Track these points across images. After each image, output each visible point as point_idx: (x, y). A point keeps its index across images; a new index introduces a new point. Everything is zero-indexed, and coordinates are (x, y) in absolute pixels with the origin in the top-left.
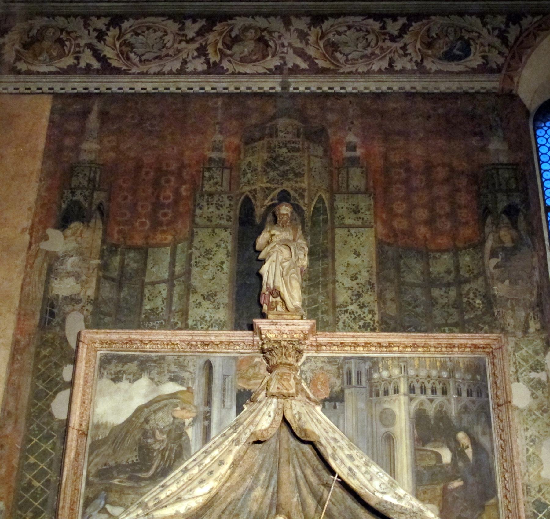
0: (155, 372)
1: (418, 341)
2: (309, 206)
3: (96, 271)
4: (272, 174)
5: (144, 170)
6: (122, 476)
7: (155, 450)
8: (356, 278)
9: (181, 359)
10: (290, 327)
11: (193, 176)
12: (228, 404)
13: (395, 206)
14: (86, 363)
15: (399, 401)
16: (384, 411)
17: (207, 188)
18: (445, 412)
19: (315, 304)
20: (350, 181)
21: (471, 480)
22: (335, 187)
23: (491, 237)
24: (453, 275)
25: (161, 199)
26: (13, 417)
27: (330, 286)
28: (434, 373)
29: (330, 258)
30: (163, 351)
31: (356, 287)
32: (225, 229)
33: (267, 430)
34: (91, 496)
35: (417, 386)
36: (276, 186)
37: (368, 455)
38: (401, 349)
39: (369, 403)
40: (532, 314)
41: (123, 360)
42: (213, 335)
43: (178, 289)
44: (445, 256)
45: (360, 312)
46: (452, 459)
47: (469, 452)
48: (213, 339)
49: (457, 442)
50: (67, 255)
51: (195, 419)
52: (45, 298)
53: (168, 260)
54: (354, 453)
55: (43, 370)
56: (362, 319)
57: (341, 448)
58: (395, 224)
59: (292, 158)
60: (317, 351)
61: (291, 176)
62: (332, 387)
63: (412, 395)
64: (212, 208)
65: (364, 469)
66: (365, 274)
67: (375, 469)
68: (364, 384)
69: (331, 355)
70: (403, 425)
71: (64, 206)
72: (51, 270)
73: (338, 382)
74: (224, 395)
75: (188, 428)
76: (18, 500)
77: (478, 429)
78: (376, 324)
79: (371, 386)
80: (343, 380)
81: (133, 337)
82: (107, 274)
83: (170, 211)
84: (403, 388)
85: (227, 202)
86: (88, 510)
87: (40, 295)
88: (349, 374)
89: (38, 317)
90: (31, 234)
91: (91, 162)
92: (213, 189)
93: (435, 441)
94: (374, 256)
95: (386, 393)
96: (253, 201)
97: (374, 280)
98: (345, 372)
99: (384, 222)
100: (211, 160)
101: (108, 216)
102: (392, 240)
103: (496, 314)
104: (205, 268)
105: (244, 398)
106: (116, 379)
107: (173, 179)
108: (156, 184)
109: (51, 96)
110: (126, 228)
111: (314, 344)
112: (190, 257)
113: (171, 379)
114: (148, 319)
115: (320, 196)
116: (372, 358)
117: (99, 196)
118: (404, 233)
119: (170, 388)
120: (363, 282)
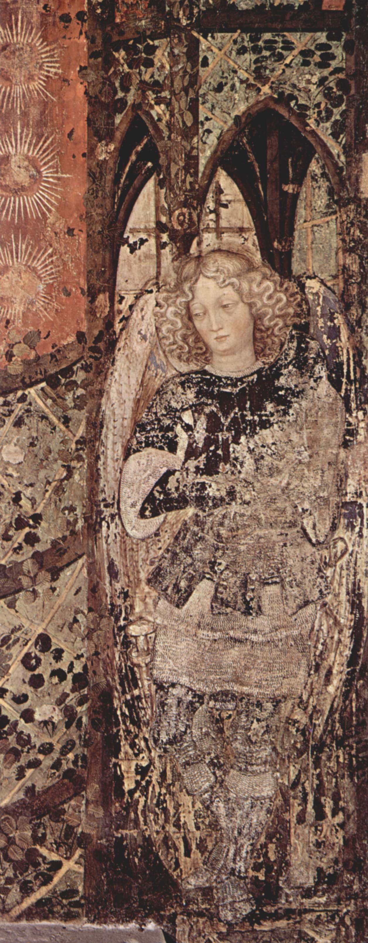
103: (128, 785)
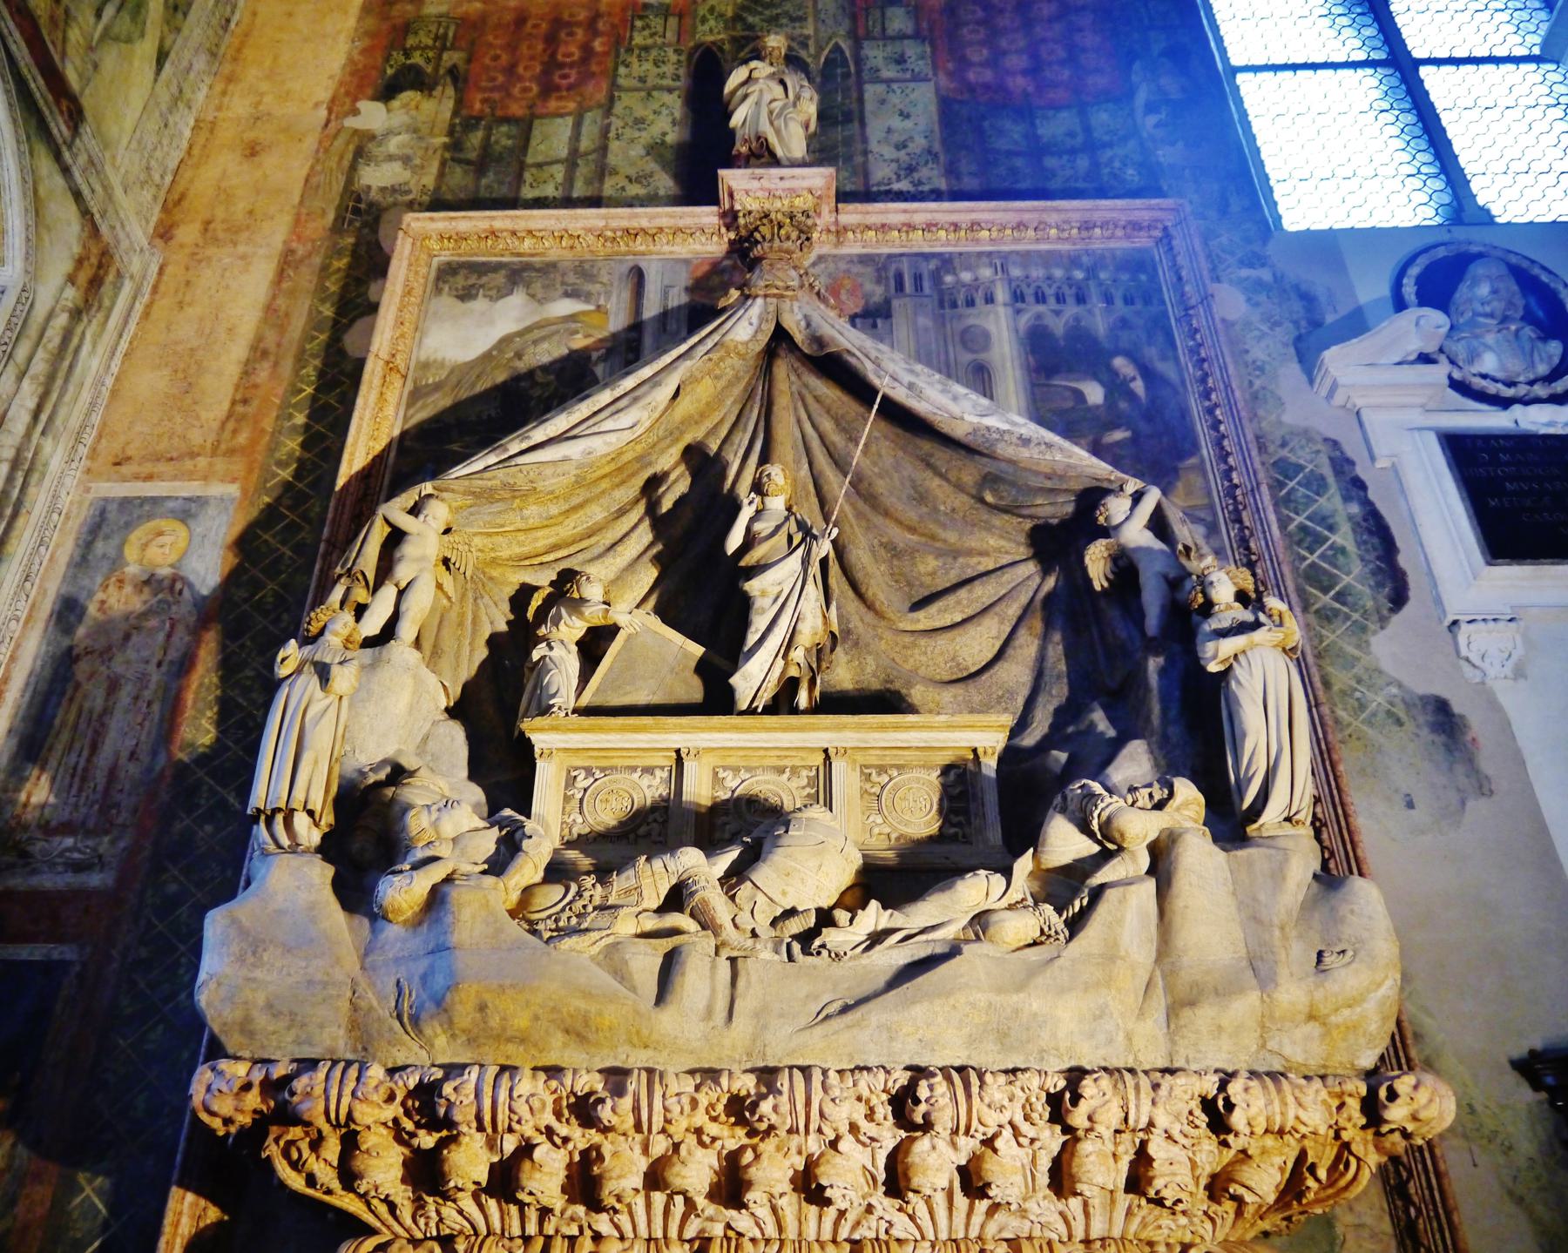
0: (537, 287)
1: (1026, 217)
2: (817, 57)
3: (439, 152)
5: (530, 24)
8: (905, 147)
9: (587, 266)
10: (787, 184)
11: (613, 26)
13: (968, 51)
14: (410, 265)
15: (996, 313)
16: (965, 331)
17: (638, 39)
20: (887, 23)
21: (1144, 427)
22: (861, 32)
24: (1080, 139)
26: (272, 358)
27: (859, 159)
29: (856, 124)
30: (554, 251)
31: (907, 158)
32: (670, 90)
33: (746, 343)
35: (1029, 293)
37: (940, 371)
38: (995, 234)
39: (941, 321)
42: (643, 217)
46: (1106, 397)
47: (1138, 386)
48: (644, 223)
53: (568, 133)
54: (919, 367)
57: (893, 360)
58: (971, 76)
63: (1019, 305)
64: (648, 66)
65: (939, 387)
67: (960, 389)
69: (865, 251)
70: (1007, 349)
71: (390, 72)
72: (359, 153)
75: (596, 364)
76: (266, 481)
77: (1151, 353)
79: (941, 293)
80: (887, 286)
81: (498, 224)
82: (461, 156)
84: (1001, 294)
85: (674, 58)
88: (899, 278)
89: (331, 216)
90: (330, 110)
91: (441, 16)
92: (650, 41)
93: (1070, 370)
94: (936, 118)
95: (971, 303)
97: (937, 147)
99: (950, 74)
101: (466, 80)
102: (966, 96)
106: (466, 295)
108: (551, 40)
110: (496, 96)
111: (833, 228)
113: (567, 295)
117: (451, 58)
118: (987, 87)
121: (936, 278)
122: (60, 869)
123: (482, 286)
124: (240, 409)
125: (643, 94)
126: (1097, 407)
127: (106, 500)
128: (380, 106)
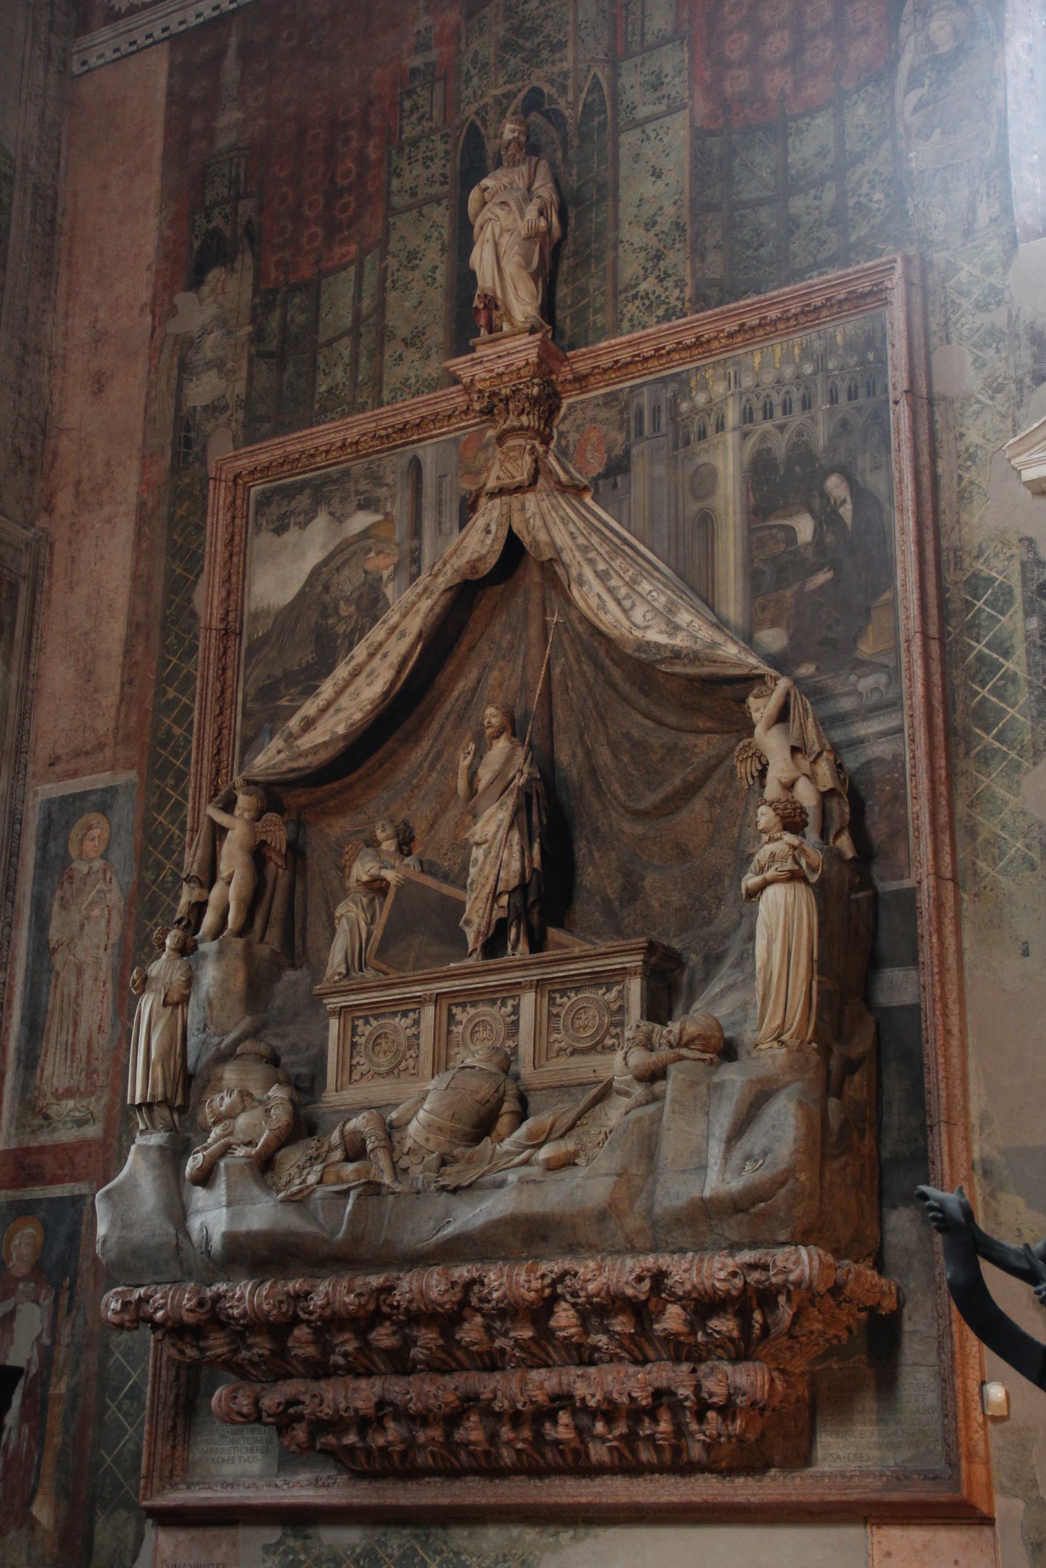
4: (514, 62)
6: (292, 691)
7: (338, 636)
8: (654, 223)
9: (374, 467)
12: (446, 525)
15: (725, 442)
17: (409, 132)
18: (806, 443)
19: (584, 297)
20: (647, 23)
23: (911, 45)
25: (339, 180)
28: (788, 372)
31: (654, 242)
32: (438, 203)
34: (250, 733)
36: (520, 84)
40: (983, 189)
41: (289, 492)
43: (366, 341)
44: (819, 121)
45: (659, 290)
47: (846, 512)
49: (824, 496)
50: (205, 331)
51: (397, 566)
52: (178, 418)
53: (351, 293)
55: (180, 541)
56: (663, 302)
59: (547, 16)
60: (584, 390)
61: (545, 55)
62: (609, 450)
63: (749, 427)
64: (418, 169)
66: (670, 210)
68: (663, 429)
70: (730, 490)
71: (197, 245)
72: (184, 367)
73: (621, 437)
74: (440, 513)
77: (864, 461)
78: (687, 304)
79: (676, 430)
83: (352, 199)
84: (732, 416)
85: (441, 148)
86: (247, 757)
87: (170, 415)
88: (640, 415)
89: (169, 454)
90: (153, 312)
96: (482, 129)
97: (686, 218)
98: (632, 415)
100: (415, 72)
104: (406, 287)
105: (468, 508)
106: (280, 529)
107: (353, 133)
109: (167, 43)
112: (383, 279)
113: (361, 507)
114: (324, 410)
115: (595, 75)
116: (678, 374)
117: (247, 209)
119: (360, 521)
120: (666, 228)
121: (674, 404)
122: (69, 1125)
123: (292, 512)
124: (127, 690)
125: (414, 212)
126: (807, 544)
127: (50, 802)
128: (191, 295)
